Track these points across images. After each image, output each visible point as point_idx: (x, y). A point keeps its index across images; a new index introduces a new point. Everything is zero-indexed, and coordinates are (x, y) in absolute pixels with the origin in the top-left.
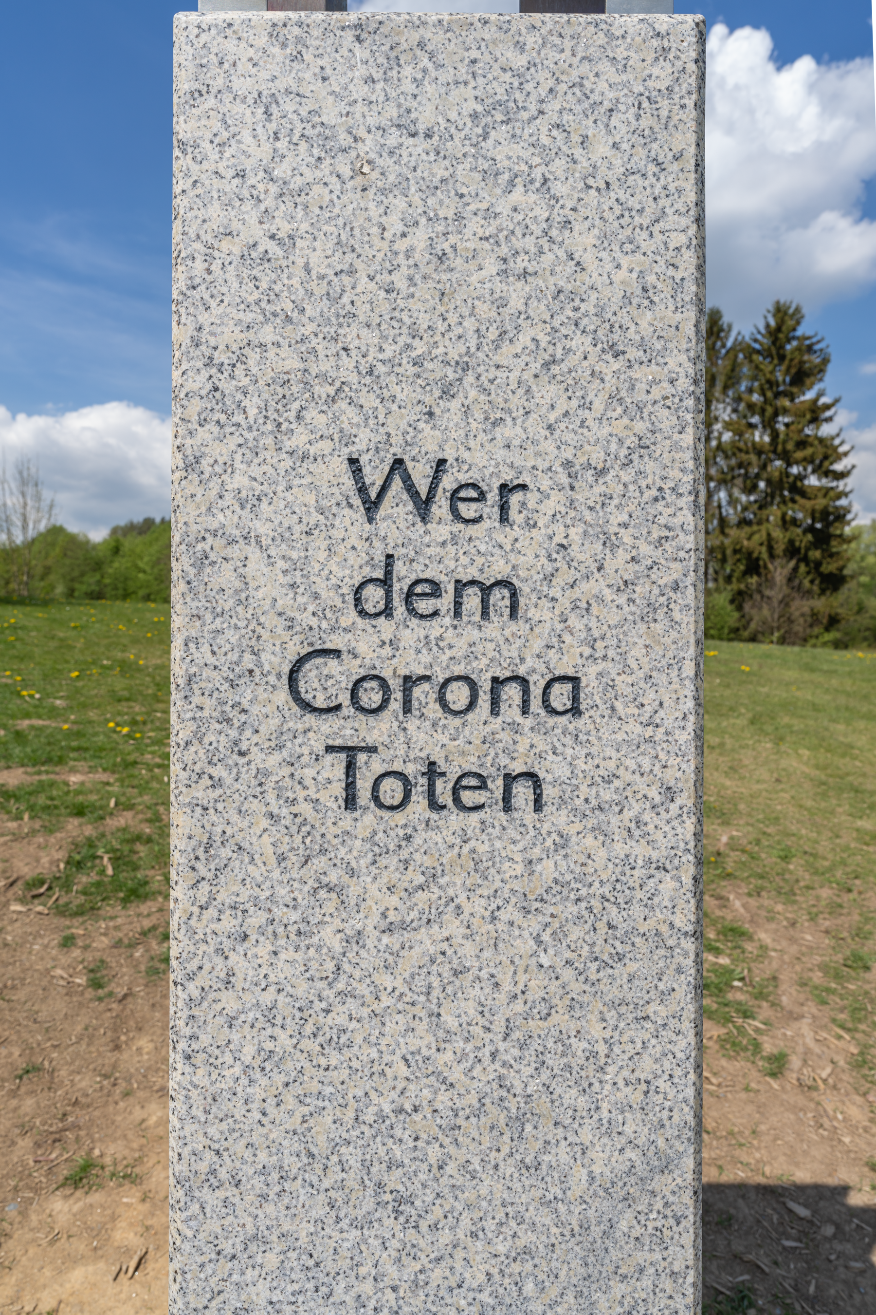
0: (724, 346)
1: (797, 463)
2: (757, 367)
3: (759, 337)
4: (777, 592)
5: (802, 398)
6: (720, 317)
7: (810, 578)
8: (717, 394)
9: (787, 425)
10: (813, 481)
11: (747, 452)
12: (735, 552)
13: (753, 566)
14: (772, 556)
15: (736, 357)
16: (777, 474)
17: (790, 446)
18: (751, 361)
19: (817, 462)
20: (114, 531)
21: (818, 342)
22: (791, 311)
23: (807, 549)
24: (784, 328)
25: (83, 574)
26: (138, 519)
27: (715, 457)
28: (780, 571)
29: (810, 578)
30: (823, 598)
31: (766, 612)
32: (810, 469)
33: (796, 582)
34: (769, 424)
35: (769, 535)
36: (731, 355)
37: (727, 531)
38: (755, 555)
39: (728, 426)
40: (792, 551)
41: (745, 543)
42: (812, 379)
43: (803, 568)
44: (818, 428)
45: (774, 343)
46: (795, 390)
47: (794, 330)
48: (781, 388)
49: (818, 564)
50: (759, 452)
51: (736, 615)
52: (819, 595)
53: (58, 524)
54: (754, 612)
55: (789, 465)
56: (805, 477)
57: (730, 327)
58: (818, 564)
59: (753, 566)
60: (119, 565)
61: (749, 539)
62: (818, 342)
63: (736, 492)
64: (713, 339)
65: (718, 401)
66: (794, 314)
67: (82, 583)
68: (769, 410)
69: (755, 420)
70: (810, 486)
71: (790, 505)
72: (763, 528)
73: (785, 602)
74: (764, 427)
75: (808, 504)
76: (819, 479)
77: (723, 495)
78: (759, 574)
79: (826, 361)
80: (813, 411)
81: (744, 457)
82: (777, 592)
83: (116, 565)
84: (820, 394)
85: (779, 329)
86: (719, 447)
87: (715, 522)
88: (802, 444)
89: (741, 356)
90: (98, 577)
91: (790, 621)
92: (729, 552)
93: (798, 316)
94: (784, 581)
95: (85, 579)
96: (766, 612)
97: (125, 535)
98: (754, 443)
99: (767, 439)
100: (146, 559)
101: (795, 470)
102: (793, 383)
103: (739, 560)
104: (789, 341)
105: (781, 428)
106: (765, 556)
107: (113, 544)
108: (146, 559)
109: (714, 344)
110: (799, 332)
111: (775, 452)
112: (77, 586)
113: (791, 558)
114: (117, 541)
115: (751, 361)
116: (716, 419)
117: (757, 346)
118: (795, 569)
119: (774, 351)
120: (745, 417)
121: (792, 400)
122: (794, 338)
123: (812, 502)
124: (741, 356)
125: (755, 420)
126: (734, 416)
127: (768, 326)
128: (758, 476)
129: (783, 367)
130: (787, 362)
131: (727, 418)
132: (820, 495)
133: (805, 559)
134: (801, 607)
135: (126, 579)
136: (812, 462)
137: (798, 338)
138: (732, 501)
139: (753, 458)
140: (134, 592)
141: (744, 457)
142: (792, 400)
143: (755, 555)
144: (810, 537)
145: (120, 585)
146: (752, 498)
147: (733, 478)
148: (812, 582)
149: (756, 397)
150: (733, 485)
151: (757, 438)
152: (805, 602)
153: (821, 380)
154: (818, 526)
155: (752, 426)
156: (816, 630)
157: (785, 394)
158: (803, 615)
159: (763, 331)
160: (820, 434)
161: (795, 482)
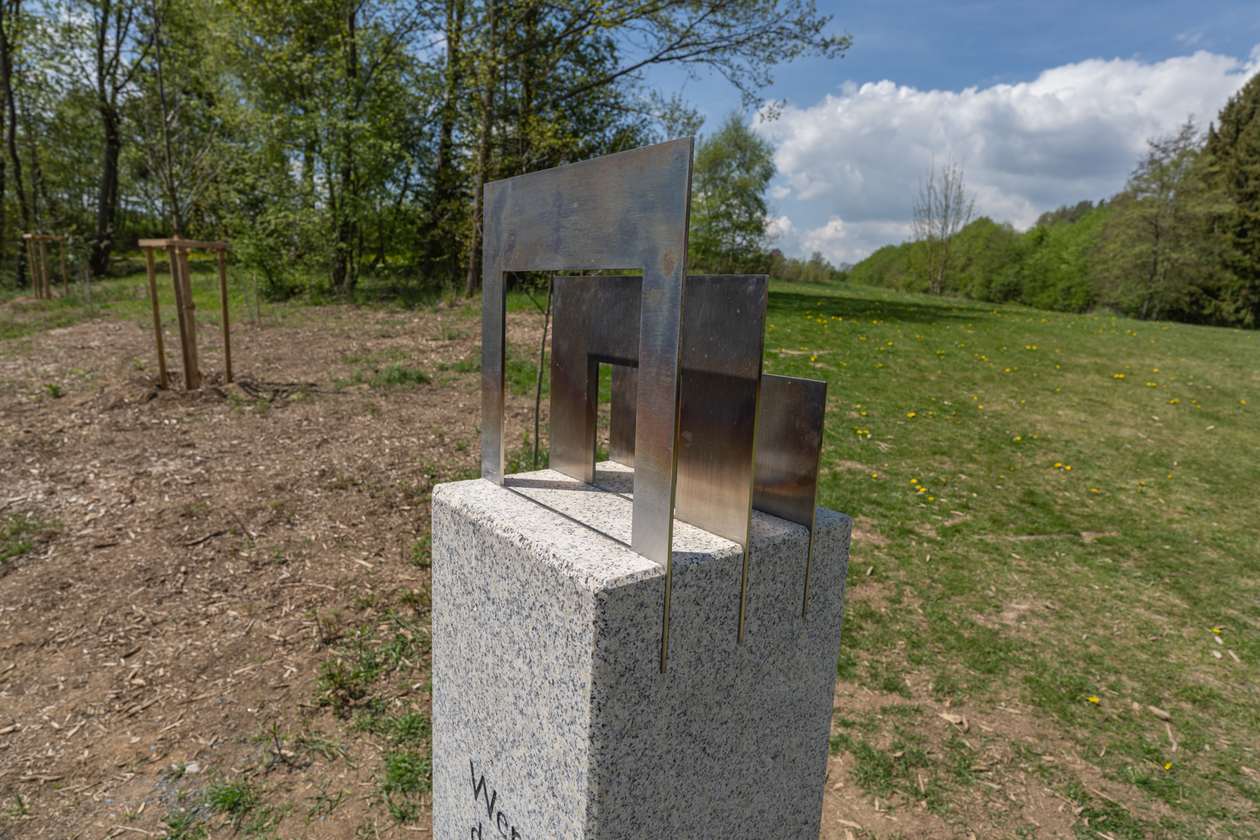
20: (1043, 219)
25: (1002, 266)
26: (1072, 203)
60: (1042, 255)
67: (1000, 274)
83: (1038, 256)
90: (1017, 267)
95: (1004, 271)
97: (1053, 224)
100: (1072, 249)
107: (1039, 234)
108: (1072, 249)
112: (995, 277)
135: (1047, 270)
140: (1053, 285)
145: (1039, 277)
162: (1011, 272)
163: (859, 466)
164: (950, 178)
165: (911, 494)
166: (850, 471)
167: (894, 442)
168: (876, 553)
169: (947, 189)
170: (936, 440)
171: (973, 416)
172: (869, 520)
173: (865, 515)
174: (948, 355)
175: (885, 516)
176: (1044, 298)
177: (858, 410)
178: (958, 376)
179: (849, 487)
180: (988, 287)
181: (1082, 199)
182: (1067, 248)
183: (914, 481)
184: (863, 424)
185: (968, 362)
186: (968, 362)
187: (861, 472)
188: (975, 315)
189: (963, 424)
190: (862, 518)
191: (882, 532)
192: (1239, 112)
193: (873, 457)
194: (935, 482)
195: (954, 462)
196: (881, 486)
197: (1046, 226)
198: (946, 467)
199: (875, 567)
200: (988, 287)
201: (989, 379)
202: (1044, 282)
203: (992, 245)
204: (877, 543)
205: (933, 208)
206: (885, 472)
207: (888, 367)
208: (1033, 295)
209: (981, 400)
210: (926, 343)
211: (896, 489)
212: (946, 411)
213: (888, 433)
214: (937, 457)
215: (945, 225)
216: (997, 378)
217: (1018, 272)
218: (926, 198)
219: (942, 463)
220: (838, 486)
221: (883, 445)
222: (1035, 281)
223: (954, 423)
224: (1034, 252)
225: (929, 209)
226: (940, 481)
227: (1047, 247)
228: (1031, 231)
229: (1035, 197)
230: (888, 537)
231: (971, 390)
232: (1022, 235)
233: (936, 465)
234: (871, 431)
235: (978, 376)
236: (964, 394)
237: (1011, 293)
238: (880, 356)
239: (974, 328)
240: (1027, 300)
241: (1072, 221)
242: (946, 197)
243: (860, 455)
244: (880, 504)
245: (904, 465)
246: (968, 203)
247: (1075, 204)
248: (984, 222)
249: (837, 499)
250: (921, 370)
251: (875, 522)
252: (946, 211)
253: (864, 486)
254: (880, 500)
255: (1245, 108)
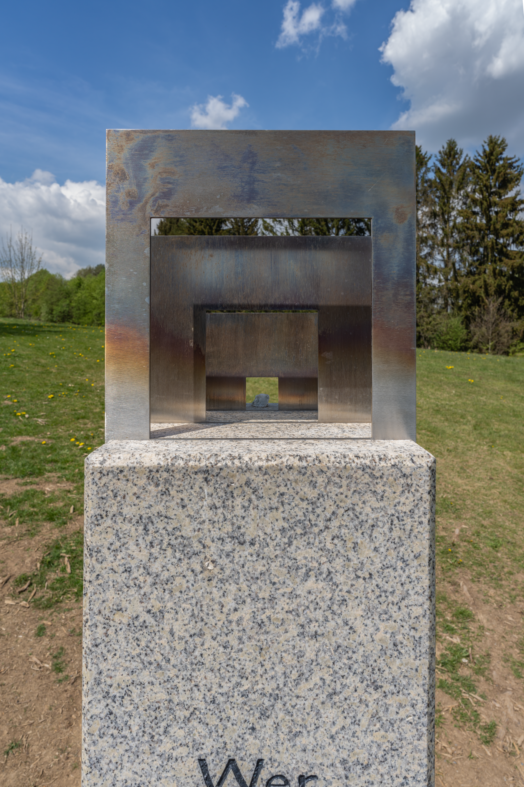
0: (458, 163)
1: (503, 237)
2: (478, 177)
3: (479, 158)
4: (490, 317)
5: (506, 196)
6: (456, 146)
7: (511, 308)
8: (453, 193)
9: (497, 213)
10: (513, 248)
11: (472, 230)
12: (465, 292)
13: (476, 300)
14: (487, 294)
15: (465, 170)
16: (490, 243)
17: (498, 226)
18: (474, 173)
19: (516, 236)
21: (516, 161)
22: (499, 142)
23: (510, 291)
24: (494, 153)
25: (58, 300)
27: (452, 233)
28: (492, 304)
29: (511, 308)
30: (520, 321)
31: (484, 329)
32: (511, 240)
33: (503, 311)
34: (486, 213)
35: (485, 281)
36: (462, 168)
37: (459, 278)
38: (477, 294)
39: (460, 213)
40: (500, 291)
41: (471, 286)
42: (512, 184)
43: (507, 302)
44: (516, 215)
45: (488, 162)
46: (501, 191)
47: (501, 154)
48: (493, 190)
49: (517, 300)
50: (480, 230)
51: (465, 331)
52: (517, 319)
53: (44, 269)
54: (477, 330)
55: (498, 237)
56: (509, 244)
57: (461, 151)
58: (517, 300)
59: (476, 301)
60: (81, 295)
61: (473, 283)
62: (516, 161)
63: (465, 254)
64: (451, 159)
65: (454, 197)
66: (501, 144)
67: (57, 305)
68: (485, 204)
69: (477, 209)
70: (511, 251)
71: (498, 263)
72: (483, 276)
73: (496, 324)
74: (482, 214)
75: (510, 262)
76: (517, 247)
77: (457, 257)
78: (480, 306)
79: (520, 174)
80: (513, 205)
81: (469, 232)
82: (490, 317)
83: (79, 295)
84: (518, 194)
85: (491, 153)
86: (454, 226)
87: (452, 273)
88: (506, 225)
89: (468, 170)
90: (68, 302)
91: (499, 335)
92: (461, 292)
93: (503, 145)
94: (495, 311)
95: (60, 303)
96: (484, 329)
97: (85, 276)
98: (476, 225)
99: (484, 221)
100: (97, 291)
101: (501, 241)
102: (500, 187)
103: (467, 297)
104: (498, 160)
105: (493, 214)
106: (483, 295)
107: (78, 281)
108: (97, 291)
109: (452, 162)
110: (504, 156)
111: (489, 229)
112: (55, 307)
113: (500, 297)
114: (80, 280)
115: (474, 173)
116: (453, 209)
117: (478, 164)
118: (502, 303)
119: (488, 168)
120: (470, 207)
121: (500, 197)
122: (501, 159)
123: (513, 261)
124: (468, 170)
125: (477, 209)
126: (464, 206)
127: (485, 151)
128: (478, 245)
129: (494, 177)
130: (496, 174)
131: (460, 208)
132: (518, 256)
133: (509, 297)
134: (506, 326)
135: (85, 303)
136: (513, 236)
137: (504, 159)
138: (462, 260)
139: (476, 233)
141: (469, 232)
142: (500, 197)
143: (477, 294)
144: (511, 282)
145: (81, 307)
146: (475, 258)
147: (464, 245)
148: (513, 311)
149: (477, 196)
150: (463, 250)
151: (478, 221)
152: (508, 324)
153: (518, 185)
154: (517, 276)
155: (474, 213)
156: (515, 341)
157: (495, 193)
158: (507, 332)
159: (482, 155)
160: (517, 219)
161: (502, 248)
162: (64, 304)
163: (29, 438)
164: (24, 242)
165: (74, 449)
166: (23, 443)
167: (46, 416)
168: (69, 495)
169: (22, 248)
170: (75, 410)
171: (91, 391)
172: (54, 474)
173: (49, 472)
174: (58, 355)
175: (64, 469)
176: (85, 319)
177: (10, 399)
178: (70, 367)
179: (29, 454)
180: (51, 314)
181: (99, 263)
182: (95, 291)
183: (73, 440)
184: (18, 409)
185: (73, 358)
186: (73, 358)
187: (32, 442)
188: (56, 329)
189: (87, 396)
190: (47, 474)
191: (68, 480)
192: (165, 227)
193: (36, 430)
194: (87, 438)
195: (93, 422)
196: (52, 449)
197: (82, 277)
198: (89, 426)
199: (75, 505)
200: (51, 314)
201: (89, 367)
202: (85, 310)
203: (50, 287)
204: (67, 488)
205: (13, 260)
206: (50, 438)
207: (19, 367)
208: (79, 318)
209: (91, 380)
210: (39, 349)
211: (63, 448)
212: (72, 391)
213: (40, 411)
214: (81, 421)
215: (23, 273)
216: (94, 366)
217: (68, 304)
218: (8, 253)
219: (85, 424)
220: (20, 456)
221: (40, 420)
222: (79, 309)
223: (81, 397)
224: (76, 293)
225: (11, 261)
226: (89, 436)
227: (83, 289)
228: (73, 280)
229: (78, 258)
230: (73, 481)
231: (82, 375)
232: (68, 281)
233: (82, 426)
234: (27, 412)
235: (83, 366)
236: (79, 378)
237: (66, 317)
238: (9, 359)
239: (65, 337)
240: (76, 321)
241: (95, 275)
242: (22, 253)
243: (26, 430)
244: (56, 462)
245: (61, 431)
246: (37, 259)
247: (96, 265)
248: (43, 272)
249: (23, 465)
250: (43, 366)
251: (59, 474)
252: (22, 263)
253: (39, 451)
254: (54, 458)
255: (167, 225)
